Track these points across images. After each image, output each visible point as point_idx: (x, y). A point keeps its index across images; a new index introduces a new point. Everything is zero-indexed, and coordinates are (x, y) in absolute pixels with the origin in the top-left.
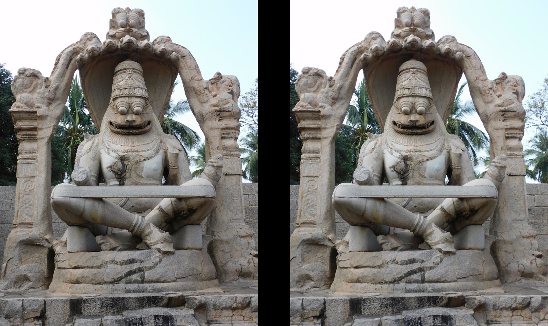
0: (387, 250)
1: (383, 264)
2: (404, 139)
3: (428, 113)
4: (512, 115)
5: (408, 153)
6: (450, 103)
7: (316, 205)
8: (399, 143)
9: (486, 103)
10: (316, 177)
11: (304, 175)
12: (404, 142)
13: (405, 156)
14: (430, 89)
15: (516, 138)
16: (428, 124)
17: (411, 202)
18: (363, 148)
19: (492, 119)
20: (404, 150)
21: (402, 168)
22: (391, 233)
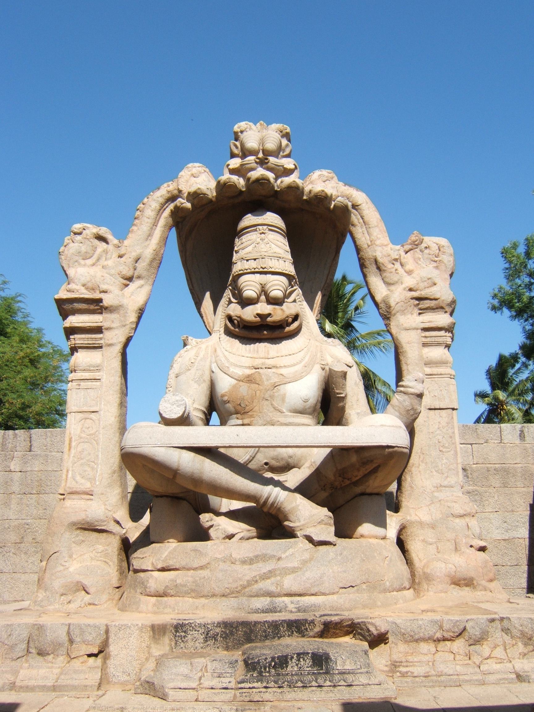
0: (218, 538)
4: (432, 305)
5: (254, 371)
6: (326, 285)
7: (93, 462)
9: (388, 284)
10: (95, 413)
11: (74, 409)
13: (249, 376)
15: (438, 344)
17: (258, 454)
18: (176, 363)
19: (398, 312)
20: (247, 365)
21: (244, 396)
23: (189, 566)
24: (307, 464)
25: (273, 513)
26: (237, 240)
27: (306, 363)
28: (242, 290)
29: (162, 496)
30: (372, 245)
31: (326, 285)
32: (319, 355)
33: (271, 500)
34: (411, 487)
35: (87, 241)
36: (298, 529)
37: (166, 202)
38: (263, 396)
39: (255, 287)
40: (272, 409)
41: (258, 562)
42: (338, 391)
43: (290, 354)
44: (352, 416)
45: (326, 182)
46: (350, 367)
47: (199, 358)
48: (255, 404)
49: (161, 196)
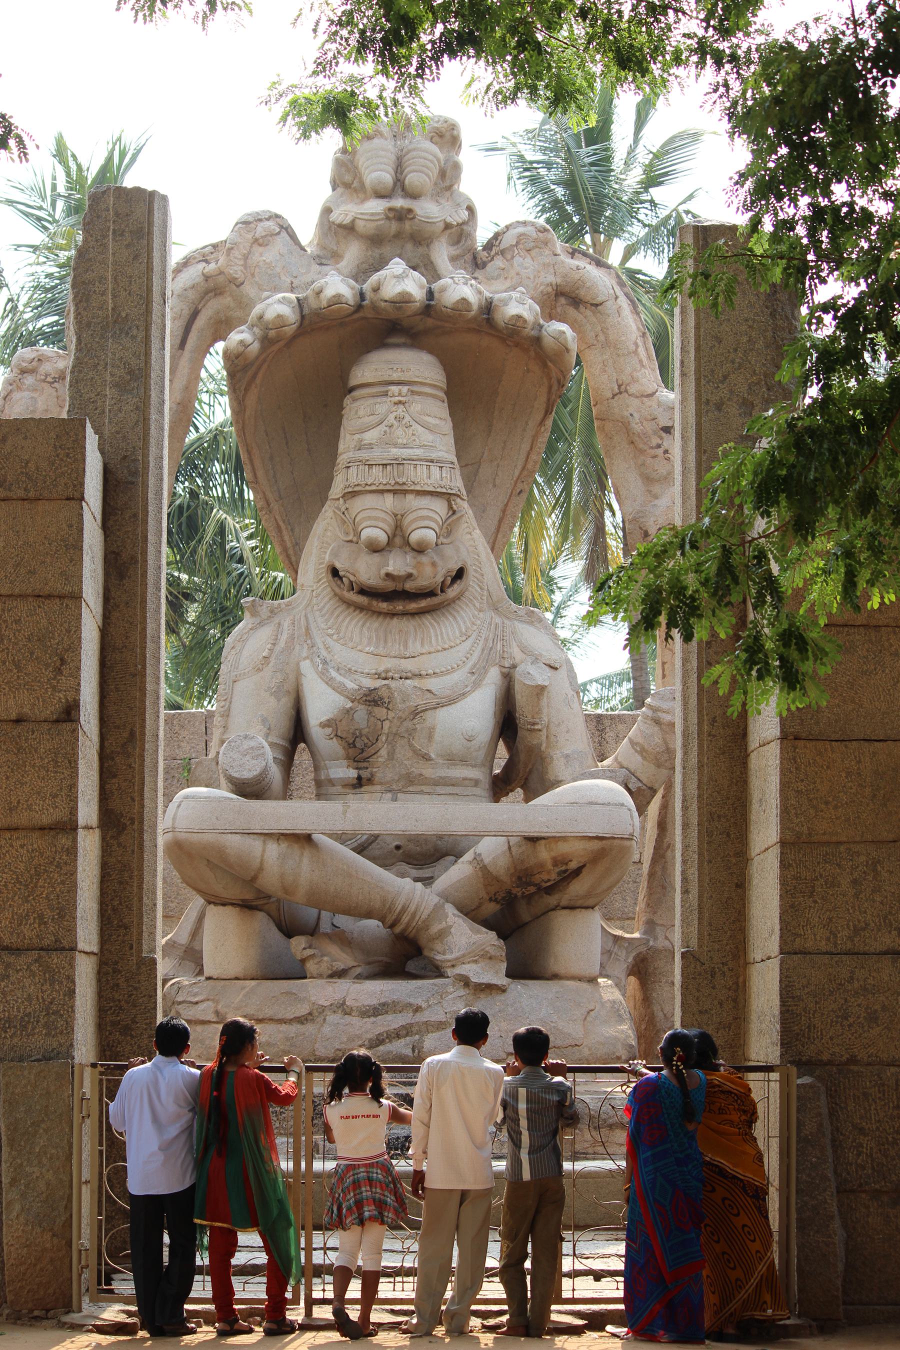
0: (320, 976)
1: (310, 1014)
2: (365, 629)
3: (445, 541)
5: (379, 683)
8: (350, 645)
9: (648, 479)
12: (365, 641)
14: (452, 463)
16: (443, 582)
18: (233, 652)
20: (366, 671)
21: (360, 730)
22: (325, 927)
23: (280, 1016)
24: (468, 856)
25: (412, 935)
26: (347, 400)
27: (474, 666)
28: (359, 524)
29: (224, 905)
30: (621, 393)
31: (525, 473)
32: (499, 647)
33: (405, 919)
34: (664, 887)
35: (46, 386)
36: (449, 964)
37: (203, 298)
38: (394, 731)
39: (384, 521)
40: (411, 754)
41: (387, 1013)
42: (530, 720)
43: (446, 646)
44: (555, 762)
45: (533, 253)
46: (556, 669)
47: (278, 649)
48: (379, 744)
49: (193, 287)
